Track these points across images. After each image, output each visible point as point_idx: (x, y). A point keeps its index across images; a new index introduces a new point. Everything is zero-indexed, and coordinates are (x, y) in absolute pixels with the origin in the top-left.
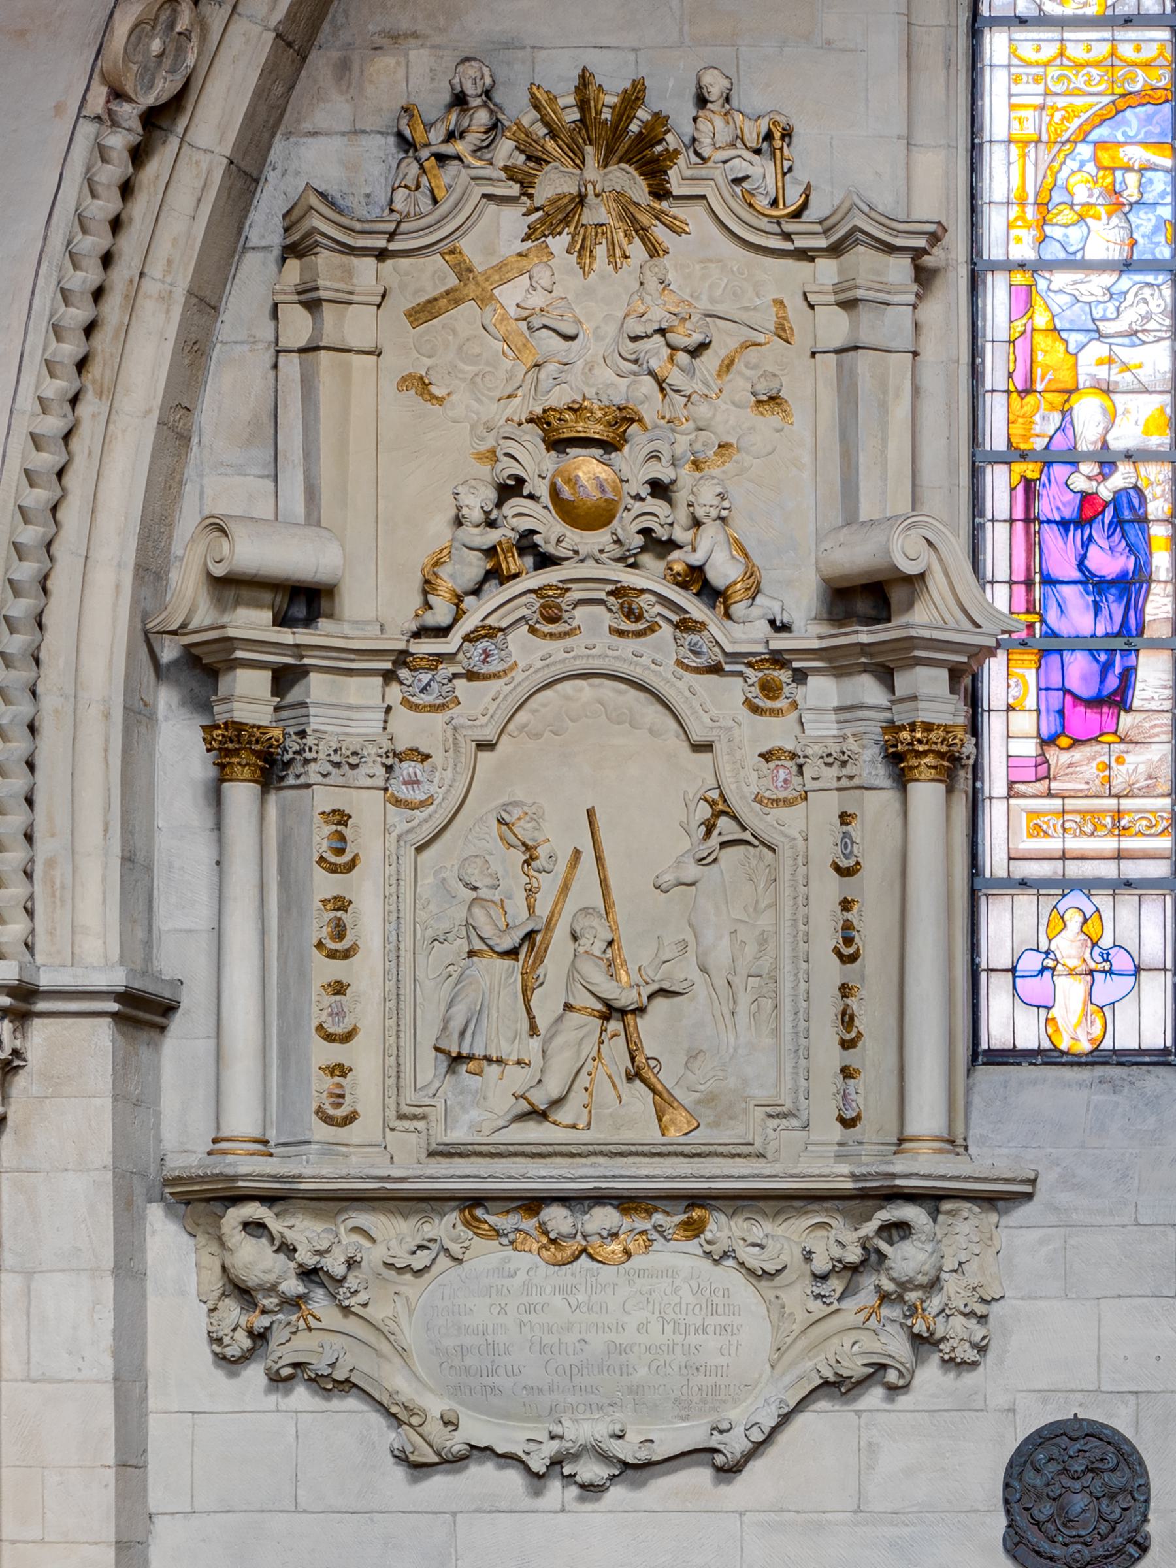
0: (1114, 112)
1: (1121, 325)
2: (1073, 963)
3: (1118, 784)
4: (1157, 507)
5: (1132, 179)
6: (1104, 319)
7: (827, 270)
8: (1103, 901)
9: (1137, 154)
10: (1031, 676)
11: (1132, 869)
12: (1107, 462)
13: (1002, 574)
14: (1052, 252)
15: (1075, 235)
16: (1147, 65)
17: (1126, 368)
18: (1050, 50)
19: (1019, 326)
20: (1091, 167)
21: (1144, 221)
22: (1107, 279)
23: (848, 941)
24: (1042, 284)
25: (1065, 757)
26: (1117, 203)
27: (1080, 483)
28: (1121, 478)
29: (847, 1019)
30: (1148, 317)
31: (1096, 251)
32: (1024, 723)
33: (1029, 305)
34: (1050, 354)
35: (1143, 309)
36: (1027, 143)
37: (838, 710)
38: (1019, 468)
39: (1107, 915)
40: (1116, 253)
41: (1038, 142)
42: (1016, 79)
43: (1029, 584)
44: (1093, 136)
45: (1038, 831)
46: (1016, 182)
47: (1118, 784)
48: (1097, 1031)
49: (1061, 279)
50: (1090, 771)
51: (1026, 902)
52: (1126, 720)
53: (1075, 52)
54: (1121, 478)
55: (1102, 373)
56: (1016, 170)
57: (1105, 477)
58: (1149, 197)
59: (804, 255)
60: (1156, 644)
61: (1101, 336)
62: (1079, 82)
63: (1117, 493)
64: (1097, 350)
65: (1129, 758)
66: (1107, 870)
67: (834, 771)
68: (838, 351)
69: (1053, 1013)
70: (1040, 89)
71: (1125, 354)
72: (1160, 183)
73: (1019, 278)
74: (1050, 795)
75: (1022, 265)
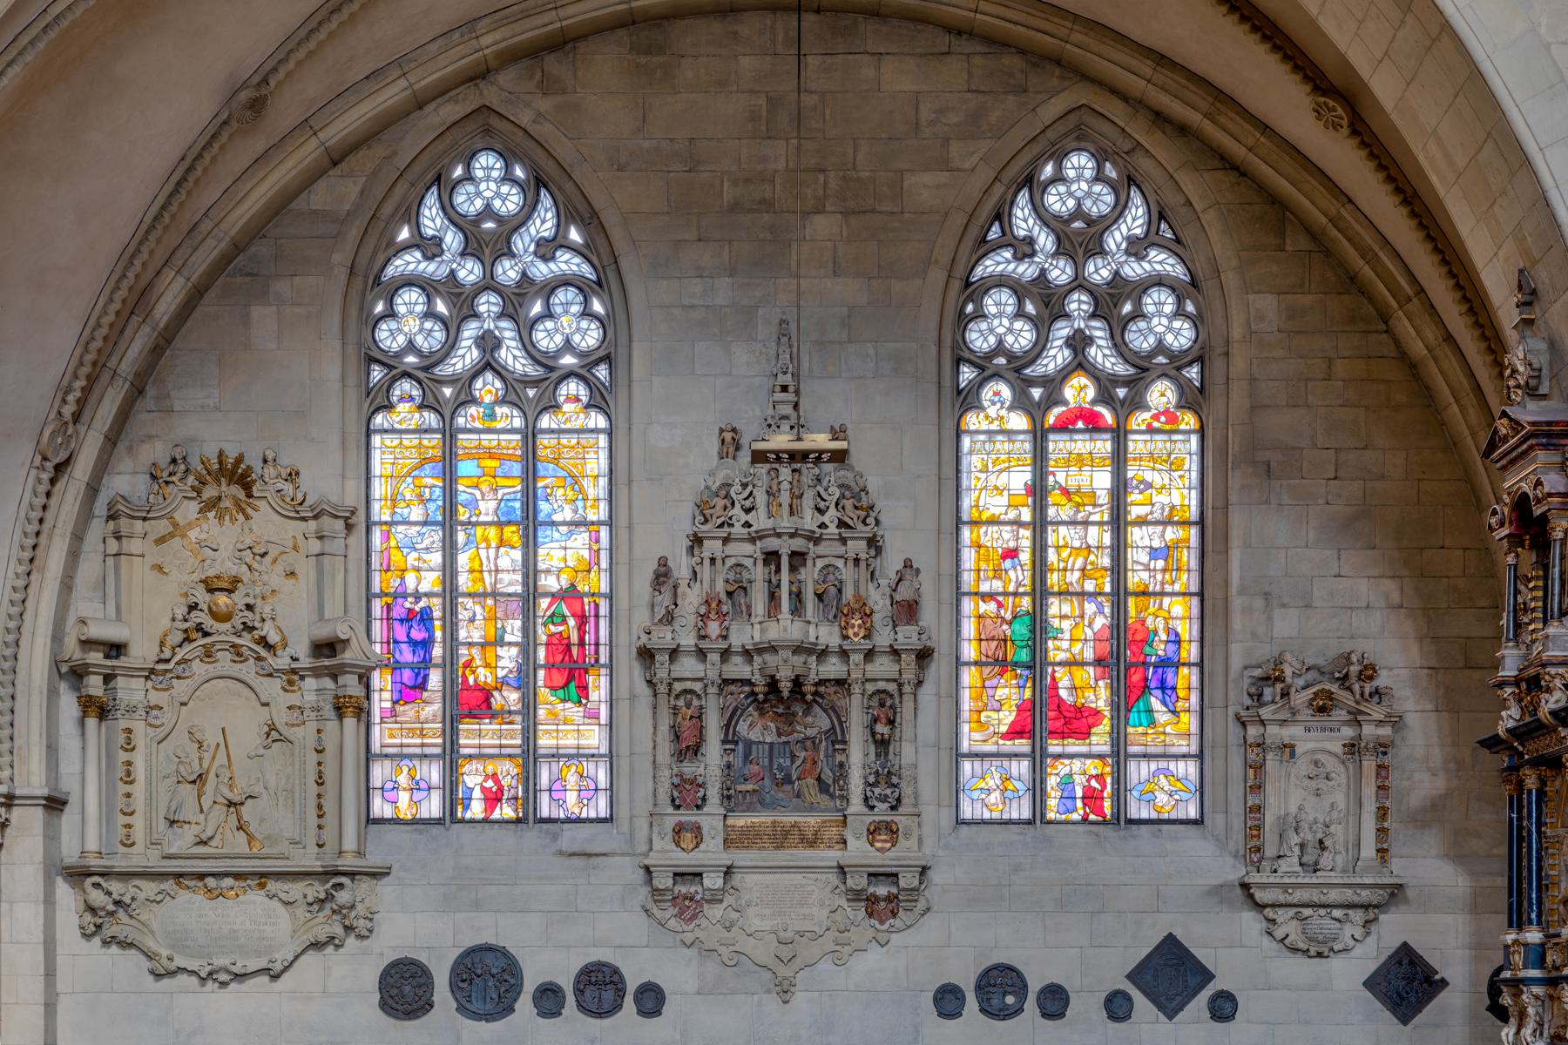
0: (420, 466)
1: (423, 546)
3: (422, 718)
4: (437, 614)
5: (427, 490)
7: (312, 525)
8: (416, 763)
9: (429, 481)
10: (389, 678)
11: (428, 751)
12: (418, 596)
13: (378, 639)
14: (398, 518)
15: (406, 511)
17: (425, 561)
18: (396, 442)
19: (384, 546)
21: (432, 506)
22: (418, 528)
23: (320, 778)
25: (402, 708)
26: (422, 500)
27: (407, 605)
28: (422, 604)
29: (320, 807)
30: (433, 542)
31: (413, 518)
32: (387, 695)
33: (388, 538)
34: (396, 556)
38: (384, 599)
40: (421, 519)
43: (388, 643)
45: (392, 736)
47: (422, 718)
48: (414, 811)
49: (400, 528)
50: (411, 713)
51: (387, 763)
52: (425, 694)
53: (406, 443)
54: (422, 604)
55: (416, 563)
56: (383, 487)
59: (304, 519)
60: (436, 666)
61: (416, 550)
62: (407, 454)
63: (422, 609)
64: (414, 555)
66: (418, 751)
67: (315, 713)
71: (425, 556)
72: (438, 492)
73: (384, 528)
74: (396, 722)
75: (386, 523)
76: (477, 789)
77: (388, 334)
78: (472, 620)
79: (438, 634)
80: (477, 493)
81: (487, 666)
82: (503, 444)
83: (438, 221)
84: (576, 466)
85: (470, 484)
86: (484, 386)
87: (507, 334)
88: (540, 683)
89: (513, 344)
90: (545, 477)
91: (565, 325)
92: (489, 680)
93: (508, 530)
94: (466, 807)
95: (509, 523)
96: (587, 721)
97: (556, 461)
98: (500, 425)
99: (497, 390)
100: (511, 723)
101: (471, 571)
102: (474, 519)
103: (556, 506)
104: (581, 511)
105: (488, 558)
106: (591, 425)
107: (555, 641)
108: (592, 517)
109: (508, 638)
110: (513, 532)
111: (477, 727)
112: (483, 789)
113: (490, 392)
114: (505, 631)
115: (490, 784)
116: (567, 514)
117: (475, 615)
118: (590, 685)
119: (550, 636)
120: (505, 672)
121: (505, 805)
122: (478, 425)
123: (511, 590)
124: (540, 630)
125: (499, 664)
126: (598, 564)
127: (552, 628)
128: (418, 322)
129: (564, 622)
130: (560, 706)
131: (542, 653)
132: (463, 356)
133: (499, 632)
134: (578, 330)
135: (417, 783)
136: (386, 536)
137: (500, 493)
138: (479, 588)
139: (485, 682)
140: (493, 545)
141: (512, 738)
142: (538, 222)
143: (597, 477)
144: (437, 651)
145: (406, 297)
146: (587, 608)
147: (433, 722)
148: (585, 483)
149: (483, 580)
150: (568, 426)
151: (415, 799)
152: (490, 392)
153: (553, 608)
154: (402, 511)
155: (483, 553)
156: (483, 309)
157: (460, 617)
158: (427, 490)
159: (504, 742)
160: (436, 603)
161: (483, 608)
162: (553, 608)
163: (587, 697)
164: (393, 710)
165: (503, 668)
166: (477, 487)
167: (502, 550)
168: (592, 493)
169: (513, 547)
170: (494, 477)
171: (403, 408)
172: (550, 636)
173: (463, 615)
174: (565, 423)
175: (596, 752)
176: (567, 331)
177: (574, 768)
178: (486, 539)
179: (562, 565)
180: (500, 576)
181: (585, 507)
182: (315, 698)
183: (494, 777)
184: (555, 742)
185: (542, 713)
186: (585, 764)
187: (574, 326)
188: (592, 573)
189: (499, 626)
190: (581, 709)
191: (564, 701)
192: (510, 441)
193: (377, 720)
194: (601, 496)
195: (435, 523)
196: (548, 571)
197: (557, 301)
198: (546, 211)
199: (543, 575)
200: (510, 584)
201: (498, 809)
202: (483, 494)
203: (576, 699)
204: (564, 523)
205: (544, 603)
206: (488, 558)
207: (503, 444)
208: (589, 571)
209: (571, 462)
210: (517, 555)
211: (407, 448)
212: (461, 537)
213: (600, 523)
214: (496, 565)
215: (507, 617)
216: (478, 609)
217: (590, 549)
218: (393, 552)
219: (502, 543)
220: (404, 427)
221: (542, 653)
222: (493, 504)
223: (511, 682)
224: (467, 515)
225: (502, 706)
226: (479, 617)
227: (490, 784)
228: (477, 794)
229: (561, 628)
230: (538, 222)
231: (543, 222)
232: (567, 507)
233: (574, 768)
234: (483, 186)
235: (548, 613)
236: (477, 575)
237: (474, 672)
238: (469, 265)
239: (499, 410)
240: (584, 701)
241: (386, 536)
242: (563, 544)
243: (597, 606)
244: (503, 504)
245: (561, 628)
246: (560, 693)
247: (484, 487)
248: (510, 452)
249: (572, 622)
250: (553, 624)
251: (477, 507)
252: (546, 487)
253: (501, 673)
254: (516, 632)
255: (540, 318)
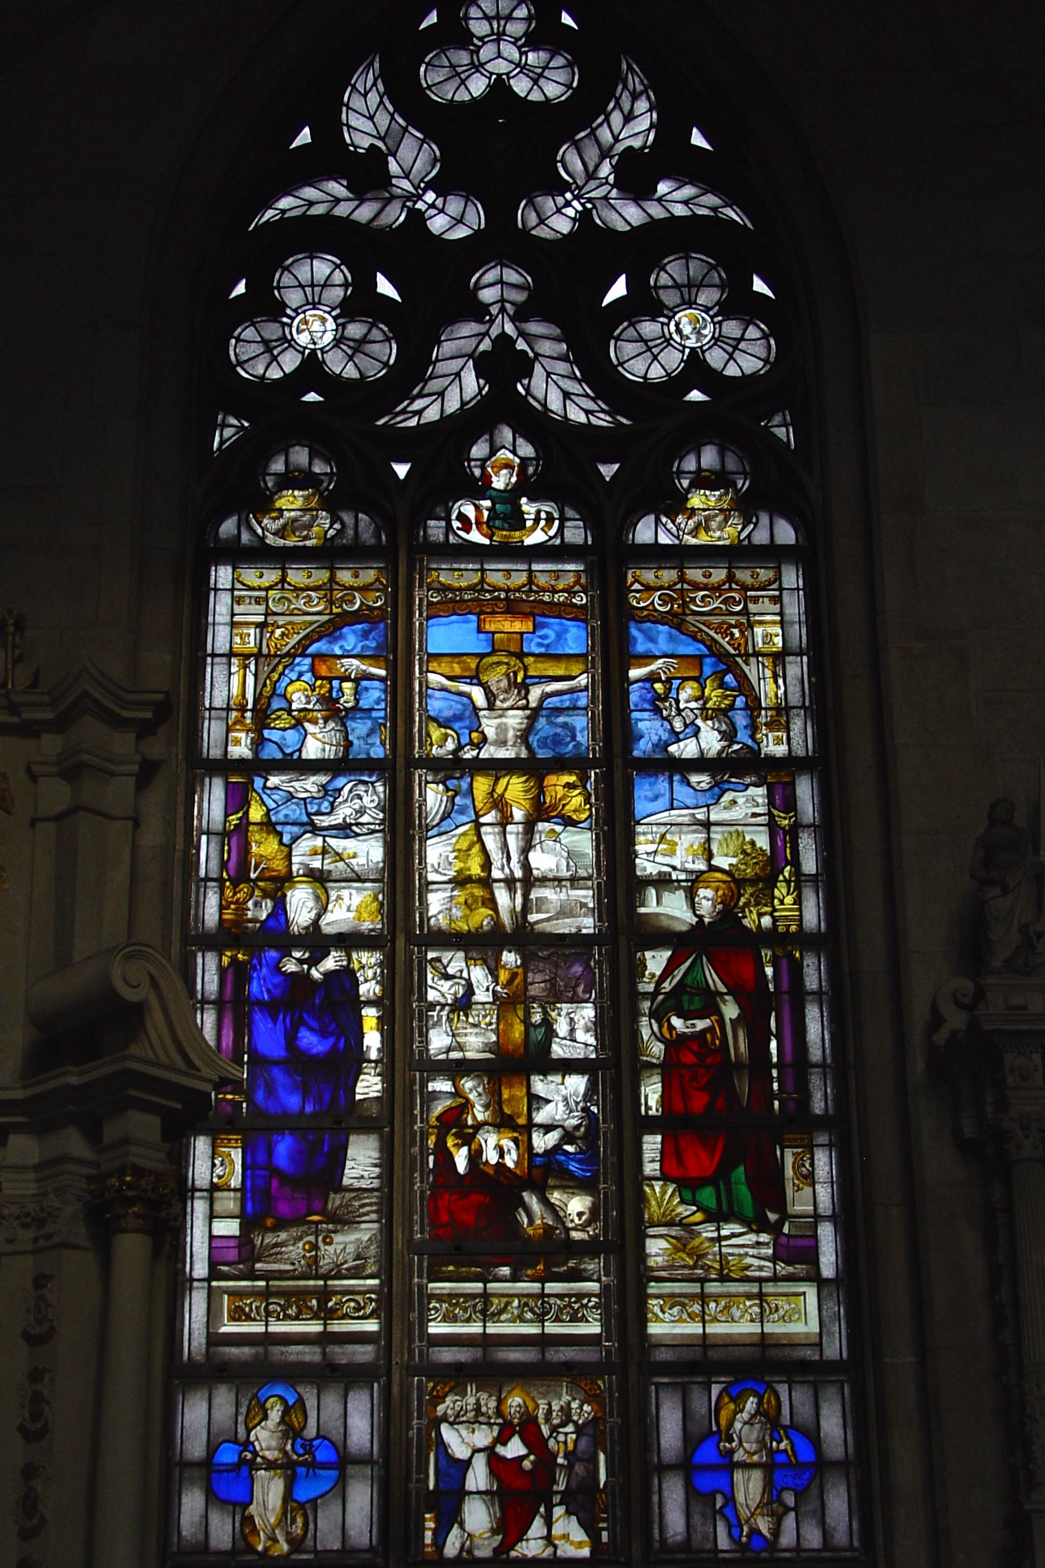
0: (332, 629)
1: (336, 819)
2: (270, 1455)
3: (325, 1263)
4: (369, 988)
5: (347, 686)
6: (319, 813)
7: (51, 744)
10: (237, 1156)
14: (270, 752)
15: (292, 736)
16: (364, 589)
17: (339, 857)
19: (234, 819)
20: (308, 677)
21: (359, 728)
23: (36, 1415)
24: (258, 782)
25: (270, 1239)
26: (332, 709)
27: (291, 967)
28: (330, 963)
29: (29, 1504)
30: (361, 811)
31: (313, 750)
32: (229, 1202)
34: (264, 847)
35: (357, 804)
36: (247, 656)
37: (37, 1168)
39: (311, 1403)
40: (330, 753)
41: (258, 656)
42: (238, 601)
44: (312, 649)
45: (238, 1315)
46: (235, 690)
47: (325, 1263)
48: (297, 1529)
50: (296, 1251)
52: (335, 1201)
54: (330, 963)
55: (316, 864)
56: (235, 681)
57: (314, 961)
58: (364, 704)
59: (30, 730)
60: (366, 1126)
61: (315, 830)
62: (300, 604)
63: (328, 975)
64: (309, 843)
65: (338, 1238)
66: (310, 1354)
67: (30, 1233)
68: (59, 818)
69: (252, 1509)
70: (261, 609)
74: (252, 1276)
75: (241, 765)
76: (480, 1461)
77: (259, 349)
78: (463, 1004)
79: (372, 1040)
80: (478, 695)
81: (503, 1122)
82: (542, 580)
83: (383, 120)
84: (725, 630)
85: (457, 670)
86: (493, 452)
87: (546, 347)
88: (651, 1168)
89: (562, 367)
90: (651, 657)
91: (687, 329)
92: (510, 1161)
93: (557, 783)
94: (450, 1516)
95: (560, 765)
96: (782, 1269)
97: (677, 621)
98: (537, 537)
99: (524, 461)
100: (576, 1275)
101: (461, 881)
102: (469, 754)
103: (678, 725)
104: (743, 736)
105: (505, 846)
106: (761, 537)
107: (688, 1058)
108: (773, 746)
109: (558, 1050)
110: (569, 786)
111: (477, 1287)
112: (496, 1463)
113: (508, 466)
114: (551, 1033)
115: (514, 1448)
116: (710, 741)
117: (470, 990)
118: (789, 1172)
119: (675, 1044)
120: (553, 1138)
121: (558, 1511)
122: (475, 536)
123: (565, 926)
124: (646, 1029)
125: (540, 1117)
126: (796, 863)
127: (677, 1022)
128: (331, 324)
129: (711, 1008)
130: (708, 1232)
131: (652, 1094)
132: (441, 394)
133: (539, 1034)
134: (717, 340)
135: (308, 1447)
136: (237, 800)
137: (535, 693)
138: (481, 917)
139: (500, 1166)
140: (518, 815)
141: (574, 1319)
142: (616, 119)
143: (779, 658)
144: (369, 1085)
145: (303, 272)
146: (769, 971)
147: (356, 1273)
148: (751, 671)
149: (491, 903)
150: (703, 539)
151: (303, 1493)
152: (508, 466)
153: (679, 974)
154: (280, 736)
155: (491, 842)
156: (488, 295)
157: (432, 995)
158: (347, 686)
159: (552, 1328)
160: (367, 960)
161: (493, 973)
162: (679, 974)
163: (780, 1205)
164: (244, 1240)
165: (548, 1128)
166: (475, 678)
167: (541, 826)
168: (769, 691)
169: (568, 822)
170: (521, 655)
171: (291, 501)
172: (675, 1044)
173: (439, 991)
174: (694, 532)
175: (811, 1354)
176: (691, 343)
177: (751, 1404)
178: (499, 803)
179: (701, 866)
180: (535, 894)
181: (753, 728)
182: (32, 1189)
183: (528, 1429)
184: (696, 1328)
185: (657, 1248)
186: (783, 1390)
187: (708, 331)
188: (780, 890)
189: (537, 1018)
190: (764, 1238)
191: (716, 1217)
192: (557, 574)
193: (201, 1270)
194: (795, 699)
195: (368, 766)
196: (663, 882)
197: (664, 279)
198: (635, 97)
199: (652, 892)
200: (564, 912)
201: (537, 1528)
202: (490, 697)
203: (749, 1212)
204: (700, 764)
205: (656, 961)
206: (505, 846)
207: (542, 580)
208: (771, 882)
209: (715, 620)
210: (583, 841)
211: (297, 589)
212: (434, 798)
213: (790, 765)
214: (526, 866)
215: (555, 996)
216: (479, 975)
217: (772, 827)
218: (255, 835)
219: (540, 811)
220: (291, 542)
221: (652, 1094)
222: (515, 720)
223: (573, 1167)
224: (450, 745)
225: (548, 1229)
226: (481, 996)
227: (514, 1448)
228: (478, 1477)
229: (701, 1024)
230: (616, 119)
231: (629, 118)
232: (705, 727)
233: (751, 1404)
234: (486, 52)
235: (667, 986)
236: (479, 892)
237: (467, 1139)
238: (455, 205)
239: (528, 508)
240: (772, 1217)
241: (237, 800)
242: (701, 815)
243: (797, 970)
244: (542, 722)
245: (701, 1024)
246: (707, 1195)
247: (496, 678)
248: (561, 597)
249: (731, 1011)
250: (685, 1016)
251: (477, 728)
252: (652, 678)
253: (542, 1142)
254: (581, 1036)
255: (628, 310)
